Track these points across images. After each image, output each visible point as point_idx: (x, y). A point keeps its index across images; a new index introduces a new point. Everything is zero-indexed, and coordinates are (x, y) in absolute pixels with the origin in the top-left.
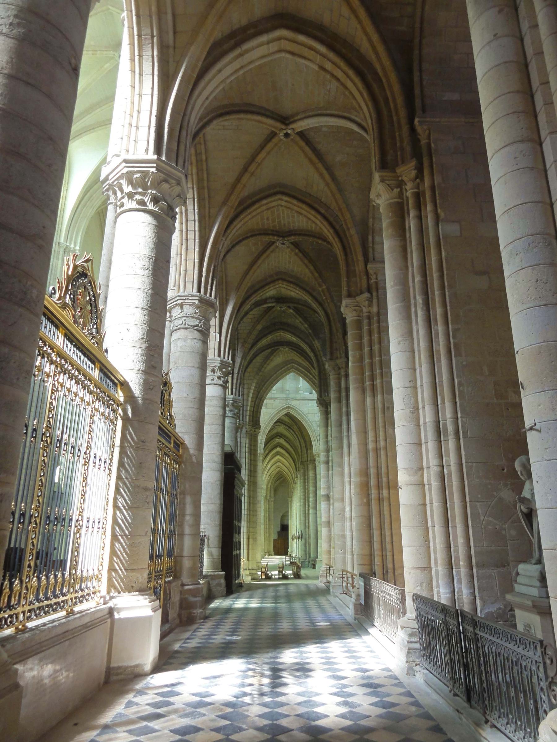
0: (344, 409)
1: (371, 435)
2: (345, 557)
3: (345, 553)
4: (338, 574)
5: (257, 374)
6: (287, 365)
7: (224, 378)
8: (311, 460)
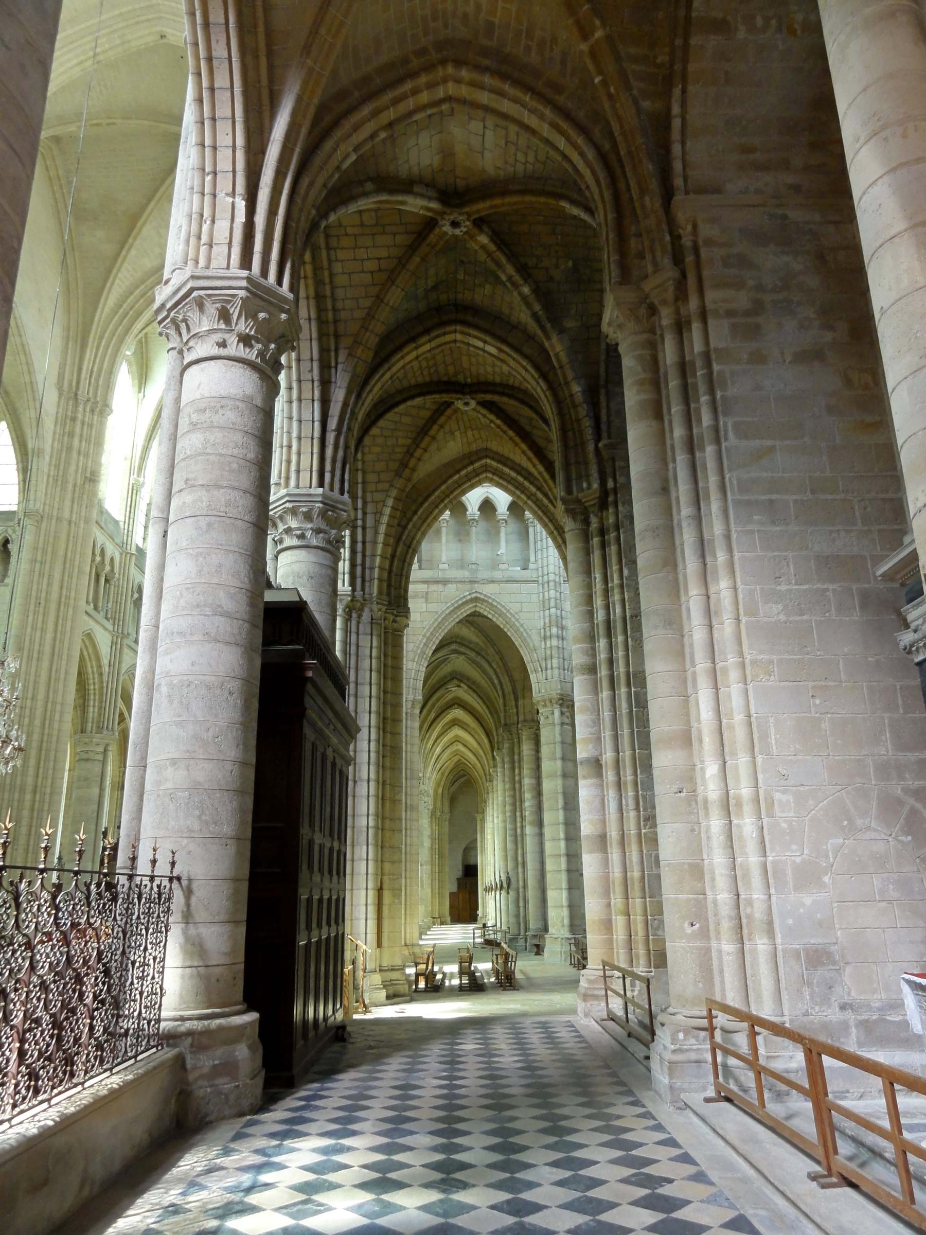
0: (679, 432)
2: (708, 950)
3: (704, 934)
5: (398, 474)
6: (472, 463)
8: (525, 721)
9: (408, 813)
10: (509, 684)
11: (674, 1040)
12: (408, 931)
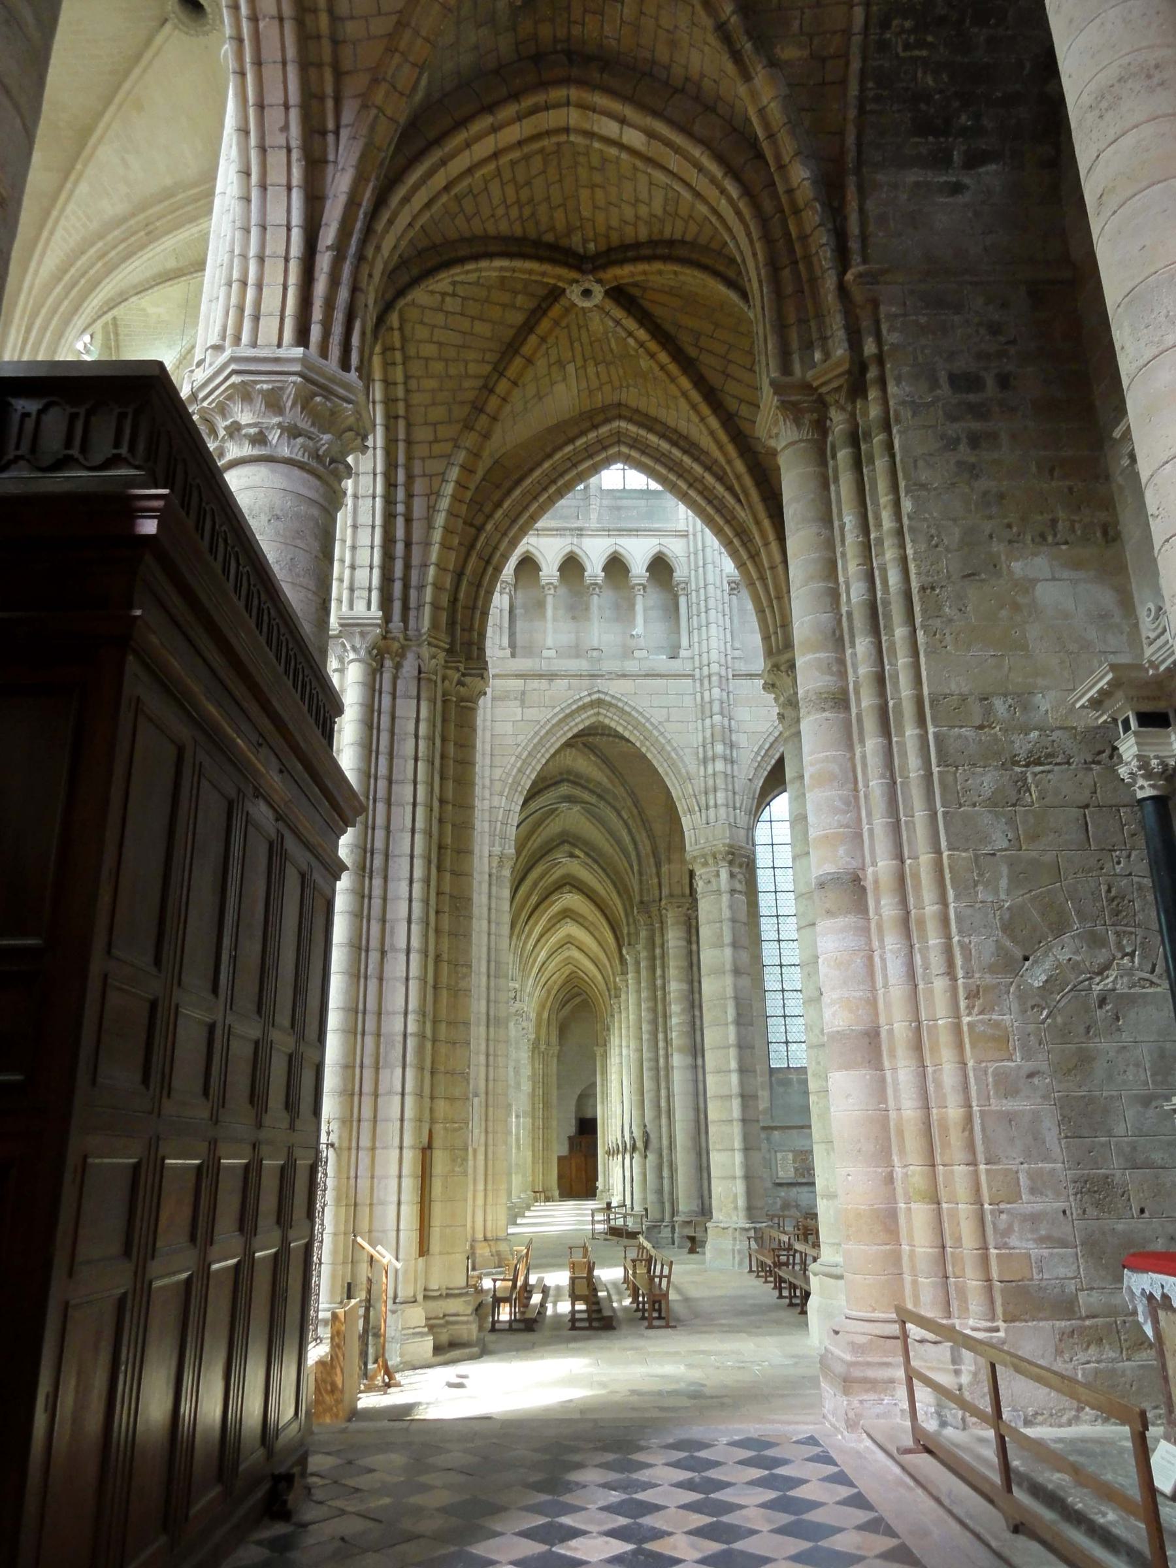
5: (468, 426)
6: (595, 427)
8: (671, 895)
9: (492, 1029)
10: (647, 842)
12: (489, 1218)
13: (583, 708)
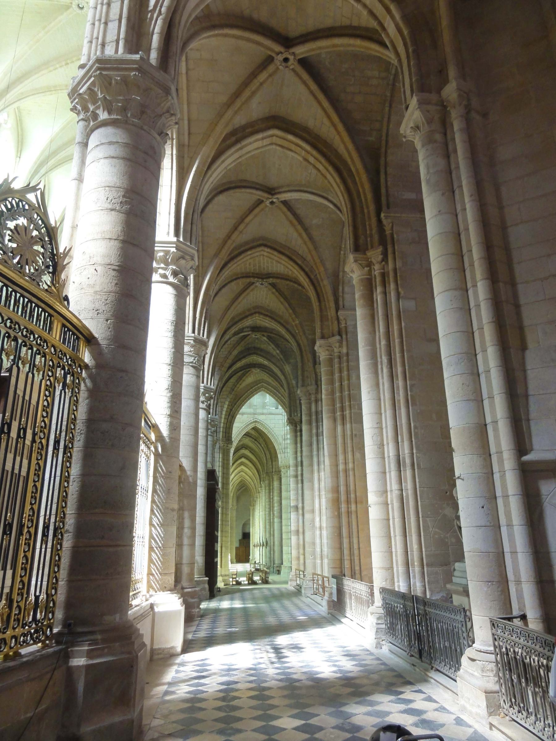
0: (314, 431)
1: (341, 458)
3: (315, 558)
4: (309, 577)
6: (257, 385)
7: (207, 402)
11: (306, 583)
13: (252, 423)
